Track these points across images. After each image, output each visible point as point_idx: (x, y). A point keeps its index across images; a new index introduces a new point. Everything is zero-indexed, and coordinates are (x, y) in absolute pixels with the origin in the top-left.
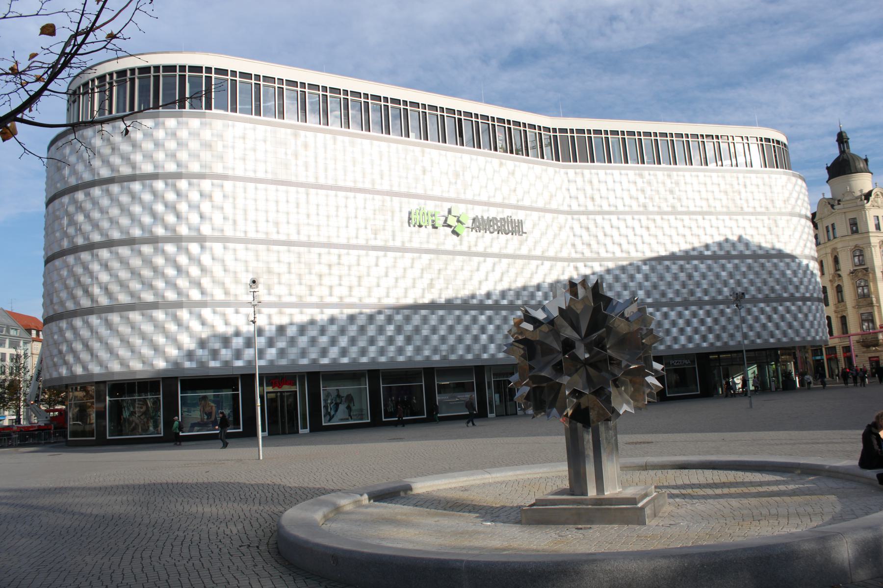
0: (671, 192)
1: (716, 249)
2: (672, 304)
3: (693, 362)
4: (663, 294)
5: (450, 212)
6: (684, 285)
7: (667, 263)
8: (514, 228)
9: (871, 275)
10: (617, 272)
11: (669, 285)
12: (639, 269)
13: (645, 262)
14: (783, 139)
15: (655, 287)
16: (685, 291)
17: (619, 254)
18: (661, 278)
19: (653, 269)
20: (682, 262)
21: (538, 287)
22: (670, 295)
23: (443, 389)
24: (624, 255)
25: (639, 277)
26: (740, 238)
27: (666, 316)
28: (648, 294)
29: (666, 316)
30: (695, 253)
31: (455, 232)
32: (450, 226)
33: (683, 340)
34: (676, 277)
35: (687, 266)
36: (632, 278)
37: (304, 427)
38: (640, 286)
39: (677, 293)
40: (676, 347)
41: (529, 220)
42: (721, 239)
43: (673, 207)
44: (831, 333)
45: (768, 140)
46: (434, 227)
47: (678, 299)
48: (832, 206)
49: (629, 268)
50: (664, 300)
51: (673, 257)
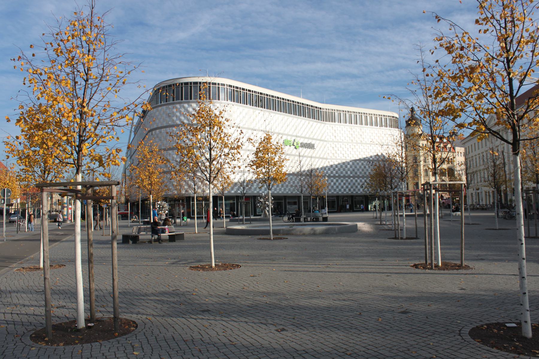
0: (361, 135)
1: (373, 157)
2: (358, 177)
3: (363, 199)
4: (356, 173)
5: (294, 140)
6: (363, 170)
7: (358, 162)
8: (310, 146)
9: (419, 168)
10: (341, 164)
11: (358, 170)
12: (348, 163)
13: (351, 161)
14: (397, 115)
15: (354, 170)
16: (363, 172)
17: (343, 158)
18: (356, 167)
19: (353, 164)
20: (362, 162)
21: (318, 169)
22: (358, 174)
23: (290, 203)
24: (344, 158)
25: (349, 166)
26: (382, 154)
27: (356, 181)
28: (351, 173)
29: (356, 181)
30: (367, 159)
31: (296, 148)
32: (294, 146)
33: (361, 190)
34: (360, 167)
35: (365, 163)
36: (346, 166)
37: (252, 215)
38: (349, 170)
39: (361, 173)
40: (359, 192)
41: (316, 143)
42: (375, 154)
43: (361, 141)
44: (408, 189)
45: (393, 117)
46: (290, 146)
47: (361, 175)
48: (407, 138)
49: (346, 163)
50: (356, 175)
51: (360, 160)
